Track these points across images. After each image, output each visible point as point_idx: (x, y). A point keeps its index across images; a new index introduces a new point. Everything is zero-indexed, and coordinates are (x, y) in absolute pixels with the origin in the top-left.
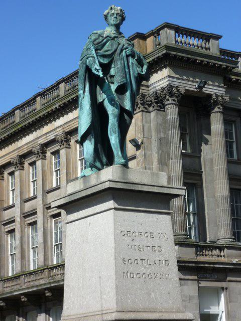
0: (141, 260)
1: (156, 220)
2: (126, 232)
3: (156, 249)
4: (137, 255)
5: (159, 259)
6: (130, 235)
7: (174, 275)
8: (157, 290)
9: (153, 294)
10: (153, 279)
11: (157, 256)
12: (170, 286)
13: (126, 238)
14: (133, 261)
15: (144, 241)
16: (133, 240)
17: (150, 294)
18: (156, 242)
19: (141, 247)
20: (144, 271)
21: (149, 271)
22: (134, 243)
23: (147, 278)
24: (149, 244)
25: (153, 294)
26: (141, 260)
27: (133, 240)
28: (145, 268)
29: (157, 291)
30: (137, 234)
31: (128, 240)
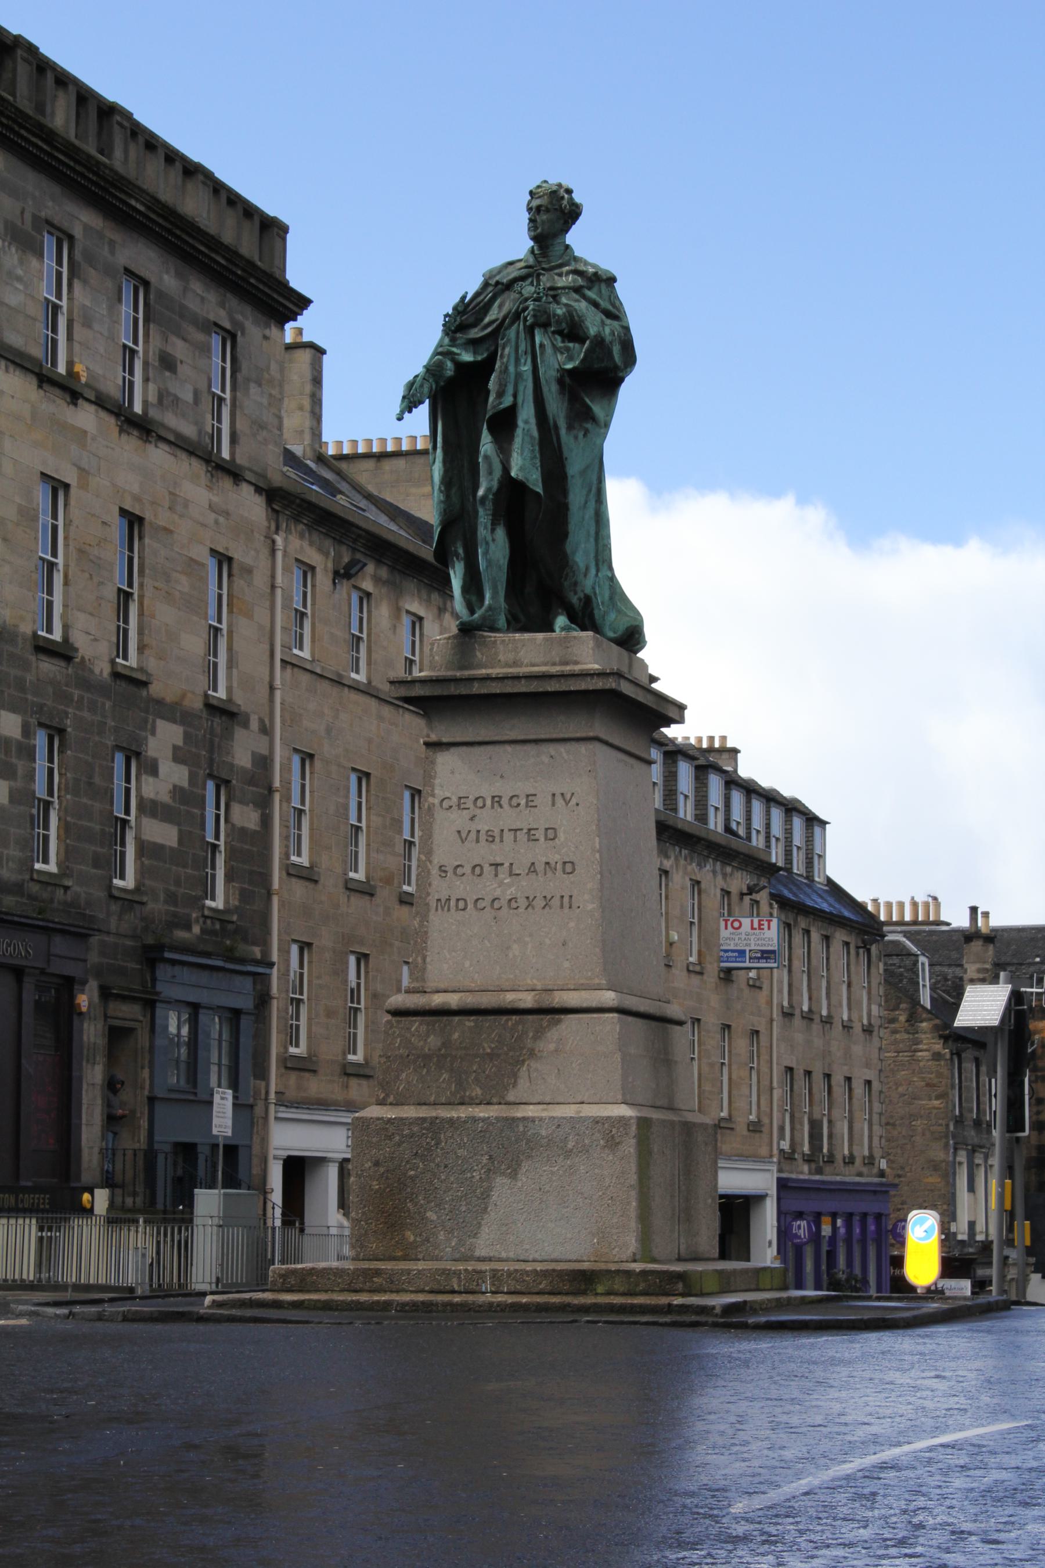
0: (491, 865)
1: (545, 759)
2: (455, 799)
3: (540, 835)
4: (483, 853)
5: (544, 859)
6: (466, 806)
7: (586, 897)
8: (531, 935)
9: (515, 946)
10: (521, 910)
11: (541, 852)
12: (572, 924)
13: (454, 815)
14: (467, 869)
15: (508, 818)
16: (472, 819)
17: (508, 948)
18: (541, 817)
19: (497, 833)
20: (498, 893)
21: (511, 892)
22: (474, 827)
23: (505, 909)
24: (518, 825)
25: (515, 946)
26: (491, 865)
27: (472, 819)
28: (501, 884)
29: (527, 939)
30: (489, 802)
31: (458, 819)
